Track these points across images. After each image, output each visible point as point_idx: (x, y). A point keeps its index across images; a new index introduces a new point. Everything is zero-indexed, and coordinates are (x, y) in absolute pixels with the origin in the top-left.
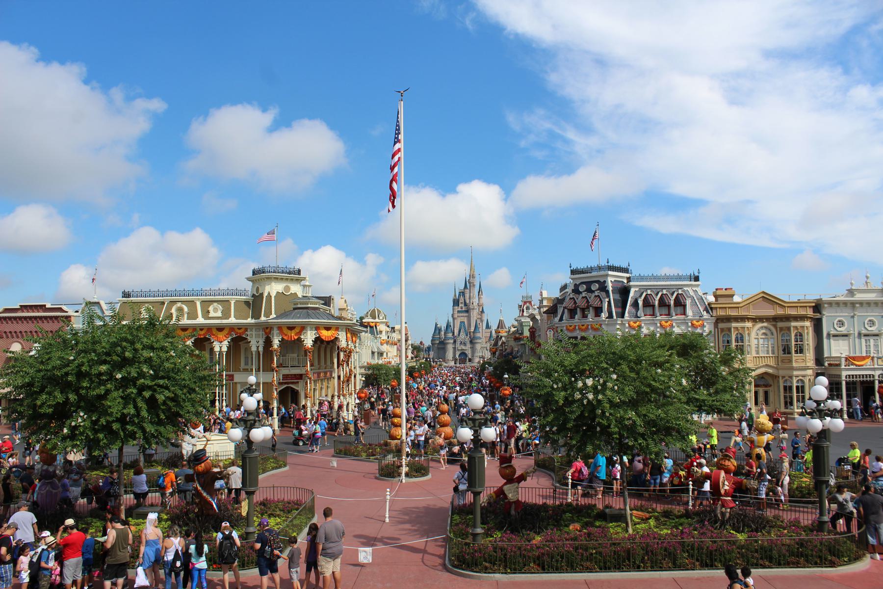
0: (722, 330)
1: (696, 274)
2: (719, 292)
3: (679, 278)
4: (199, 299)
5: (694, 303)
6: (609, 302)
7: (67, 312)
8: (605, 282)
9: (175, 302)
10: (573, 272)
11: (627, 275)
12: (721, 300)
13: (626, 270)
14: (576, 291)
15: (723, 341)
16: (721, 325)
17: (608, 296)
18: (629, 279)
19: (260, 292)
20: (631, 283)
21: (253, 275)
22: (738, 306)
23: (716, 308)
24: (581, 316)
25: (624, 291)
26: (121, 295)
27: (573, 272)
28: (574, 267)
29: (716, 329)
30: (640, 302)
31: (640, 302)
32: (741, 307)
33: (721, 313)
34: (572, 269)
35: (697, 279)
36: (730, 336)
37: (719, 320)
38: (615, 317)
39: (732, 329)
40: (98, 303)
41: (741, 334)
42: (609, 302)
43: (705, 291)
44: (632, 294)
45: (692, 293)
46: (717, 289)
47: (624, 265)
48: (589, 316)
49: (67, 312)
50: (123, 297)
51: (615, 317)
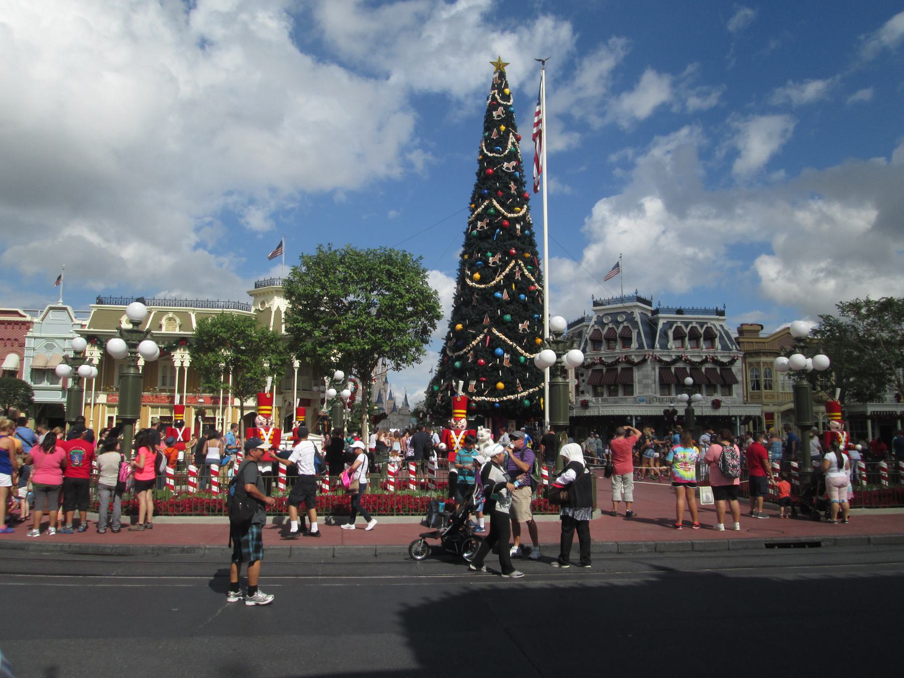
0: (751, 364)
1: (722, 309)
2: (745, 328)
3: (706, 312)
4: (194, 310)
5: (721, 338)
6: (639, 334)
7: (25, 317)
8: (632, 313)
9: (167, 312)
10: (596, 304)
11: (653, 308)
12: (746, 335)
13: (649, 303)
14: (600, 322)
15: (752, 376)
16: (749, 360)
17: (638, 328)
18: (656, 312)
19: (267, 306)
20: (660, 315)
21: (256, 287)
22: (763, 341)
23: (744, 342)
24: (607, 348)
25: (651, 325)
26: (95, 300)
27: (596, 304)
28: (597, 298)
29: (744, 364)
30: (670, 334)
31: (670, 334)
32: (767, 342)
33: (747, 347)
34: (595, 300)
35: (722, 313)
36: (758, 370)
37: (748, 354)
38: (646, 348)
39: (761, 363)
40: (65, 309)
41: (769, 368)
42: (639, 334)
43: (731, 325)
44: (660, 326)
45: (719, 328)
46: (742, 325)
47: (648, 298)
48: (617, 347)
49: (25, 317)
50: (97, 303)
51: (646, 348)
